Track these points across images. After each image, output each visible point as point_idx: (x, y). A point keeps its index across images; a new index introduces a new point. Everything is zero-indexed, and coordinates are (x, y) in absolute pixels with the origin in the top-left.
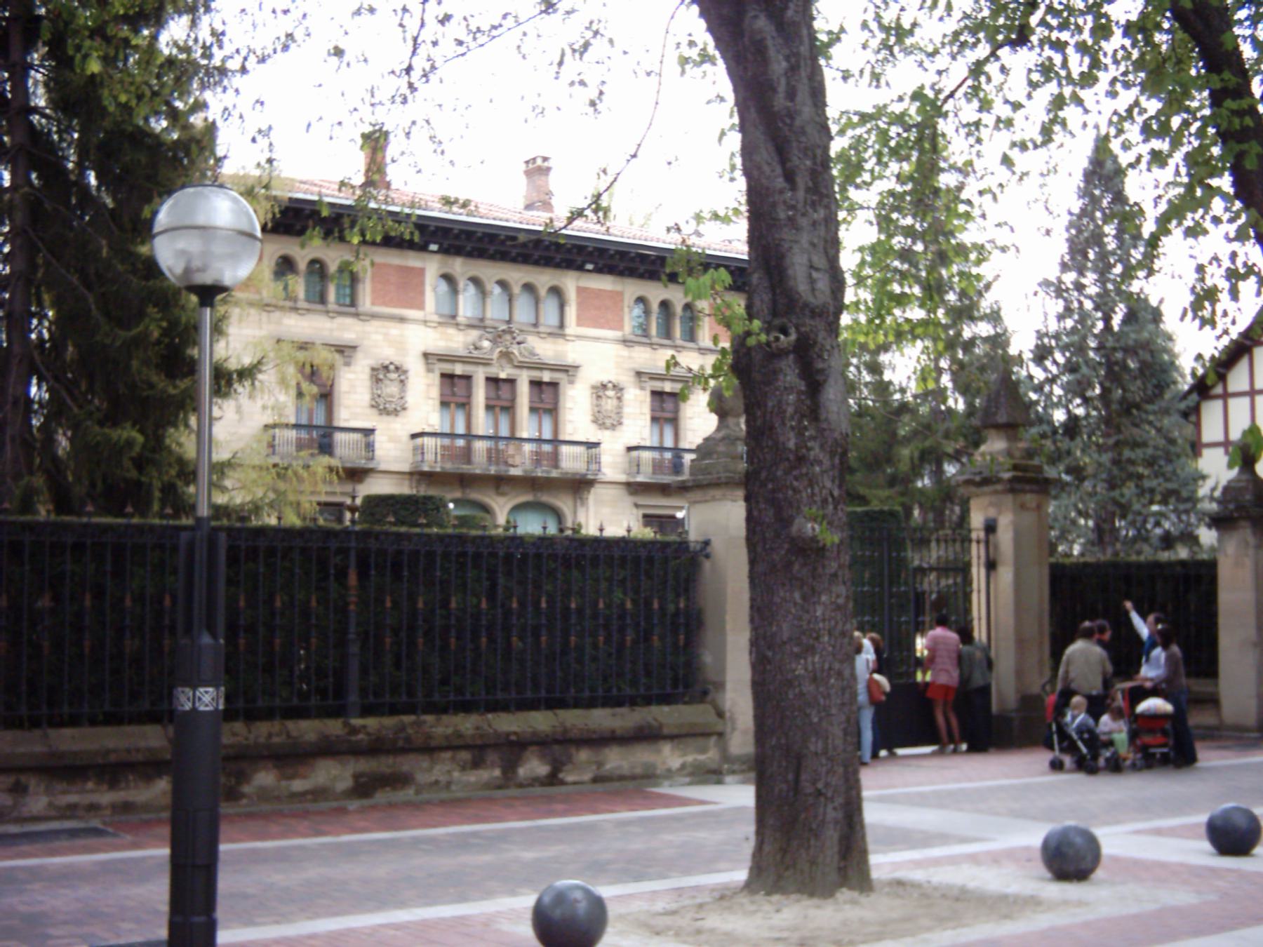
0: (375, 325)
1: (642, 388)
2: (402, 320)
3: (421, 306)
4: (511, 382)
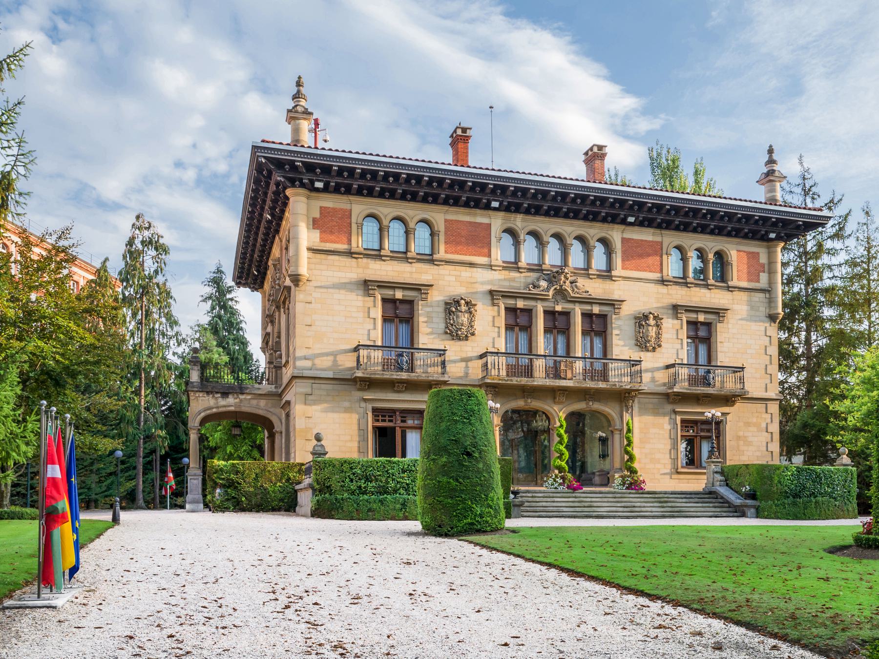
4: (566, 314)
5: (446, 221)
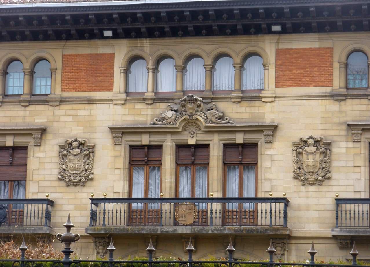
0: (65, 108)
1: (356, 141)
2: (90, 101)
3: (110, 88)
5: (64, 56)
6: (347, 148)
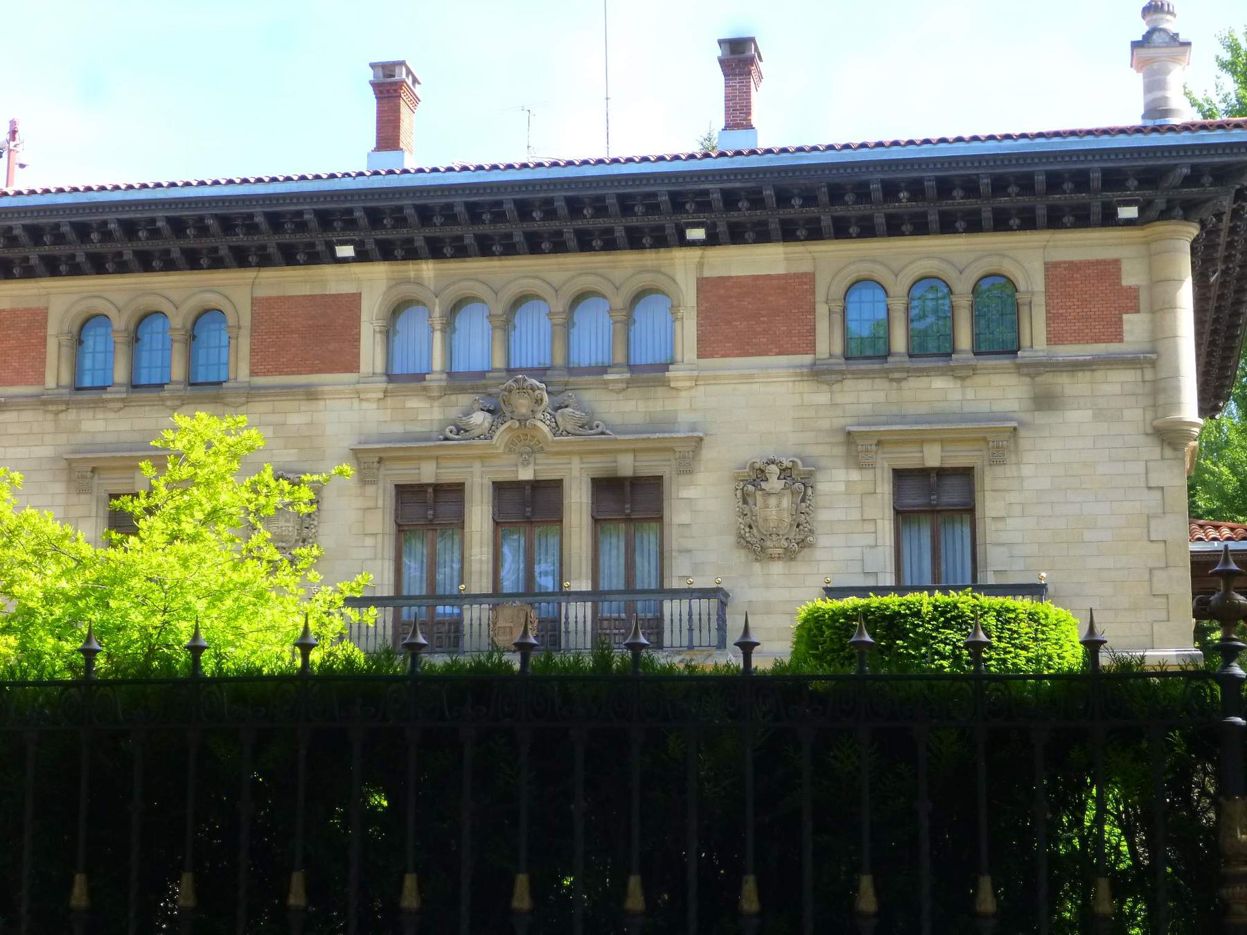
2: (311, 394)
3: (352, 365)
6: (848, 483)
